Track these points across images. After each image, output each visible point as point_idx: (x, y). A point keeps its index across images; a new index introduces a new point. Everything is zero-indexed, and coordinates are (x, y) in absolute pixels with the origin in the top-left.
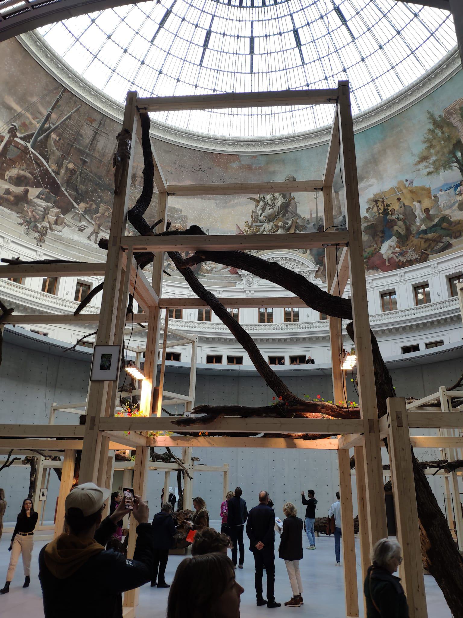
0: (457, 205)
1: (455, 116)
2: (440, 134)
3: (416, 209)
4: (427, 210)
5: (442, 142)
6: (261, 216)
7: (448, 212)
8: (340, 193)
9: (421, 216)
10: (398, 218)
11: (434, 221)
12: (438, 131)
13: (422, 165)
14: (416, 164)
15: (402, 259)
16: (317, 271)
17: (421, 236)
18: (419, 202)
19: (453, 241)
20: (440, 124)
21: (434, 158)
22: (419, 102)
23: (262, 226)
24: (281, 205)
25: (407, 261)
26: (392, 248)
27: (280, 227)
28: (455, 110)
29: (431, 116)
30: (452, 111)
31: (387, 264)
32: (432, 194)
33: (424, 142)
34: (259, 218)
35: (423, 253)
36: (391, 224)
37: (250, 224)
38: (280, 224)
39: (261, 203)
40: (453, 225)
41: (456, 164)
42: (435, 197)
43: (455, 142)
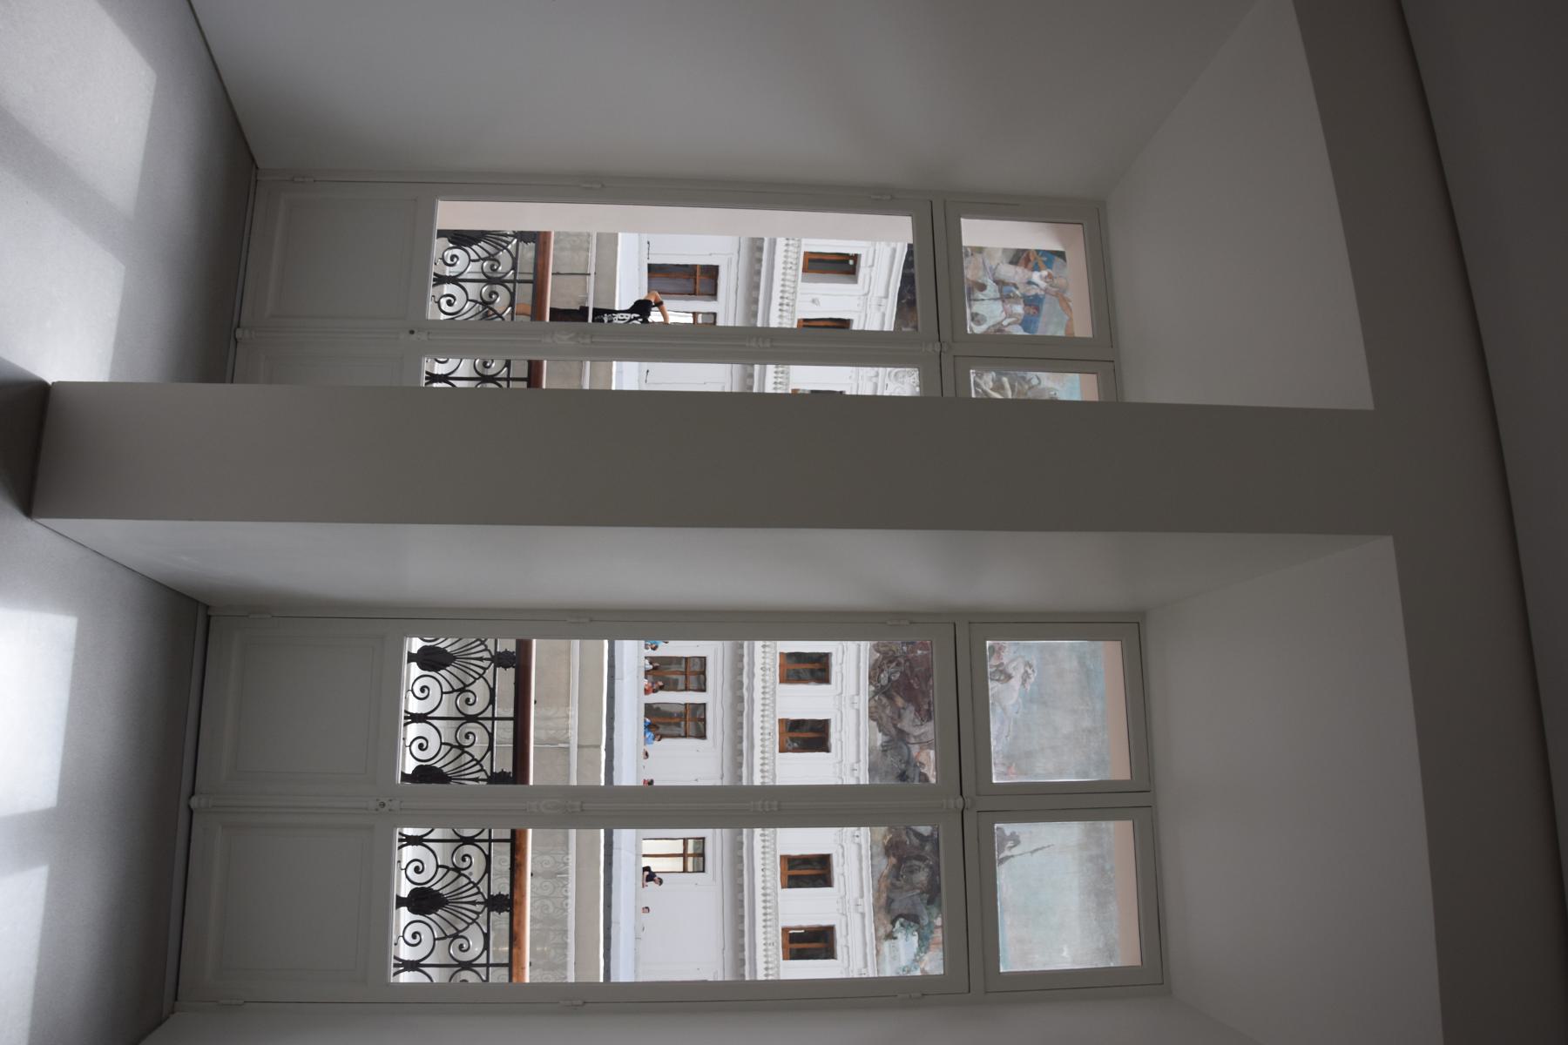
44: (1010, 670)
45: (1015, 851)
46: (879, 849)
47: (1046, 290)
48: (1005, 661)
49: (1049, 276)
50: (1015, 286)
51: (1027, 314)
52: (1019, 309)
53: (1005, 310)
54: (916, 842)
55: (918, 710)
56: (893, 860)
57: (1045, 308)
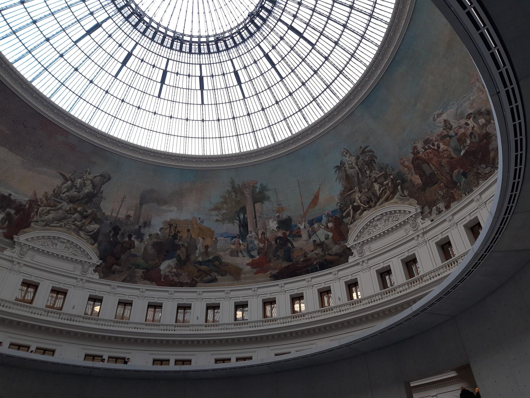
0: (229, 251)
1: (248, 190)
2: (234, 197)
3: (199, 243)
4: (207, 247)
6: (64, 193)
7: (221, 254)
8: (144, 206)
10: (183, 245)
12: (233, 194)
13: (214, 213)
14: (210, 210)
15: (176, 279)
16: (98, 266)
17: (196, 265)
18: (203, 239)
19: (219, 277)
20: (236, 190)
21: (224, 211)
22: (228, 169)
23: (61, 203)
24: (88, 193)
25: (180, 282)
26: (170, 268)
27: (78, 212)
29: (233, 183)
31: (162, 280)
32: (215, 236)
33: (221, 197)
34: (61, 195)
35: (193, 279)
36: (178, 247)
37: (49, 196)
38: (79, 209)
39: (69, 183)
41: (237, 222)
42: (216, 239)
44: (442, 124)
47: (305, 222)
50: (308, 231)
51: (317, 222)
52: (316, 226)
53: (319, 230)
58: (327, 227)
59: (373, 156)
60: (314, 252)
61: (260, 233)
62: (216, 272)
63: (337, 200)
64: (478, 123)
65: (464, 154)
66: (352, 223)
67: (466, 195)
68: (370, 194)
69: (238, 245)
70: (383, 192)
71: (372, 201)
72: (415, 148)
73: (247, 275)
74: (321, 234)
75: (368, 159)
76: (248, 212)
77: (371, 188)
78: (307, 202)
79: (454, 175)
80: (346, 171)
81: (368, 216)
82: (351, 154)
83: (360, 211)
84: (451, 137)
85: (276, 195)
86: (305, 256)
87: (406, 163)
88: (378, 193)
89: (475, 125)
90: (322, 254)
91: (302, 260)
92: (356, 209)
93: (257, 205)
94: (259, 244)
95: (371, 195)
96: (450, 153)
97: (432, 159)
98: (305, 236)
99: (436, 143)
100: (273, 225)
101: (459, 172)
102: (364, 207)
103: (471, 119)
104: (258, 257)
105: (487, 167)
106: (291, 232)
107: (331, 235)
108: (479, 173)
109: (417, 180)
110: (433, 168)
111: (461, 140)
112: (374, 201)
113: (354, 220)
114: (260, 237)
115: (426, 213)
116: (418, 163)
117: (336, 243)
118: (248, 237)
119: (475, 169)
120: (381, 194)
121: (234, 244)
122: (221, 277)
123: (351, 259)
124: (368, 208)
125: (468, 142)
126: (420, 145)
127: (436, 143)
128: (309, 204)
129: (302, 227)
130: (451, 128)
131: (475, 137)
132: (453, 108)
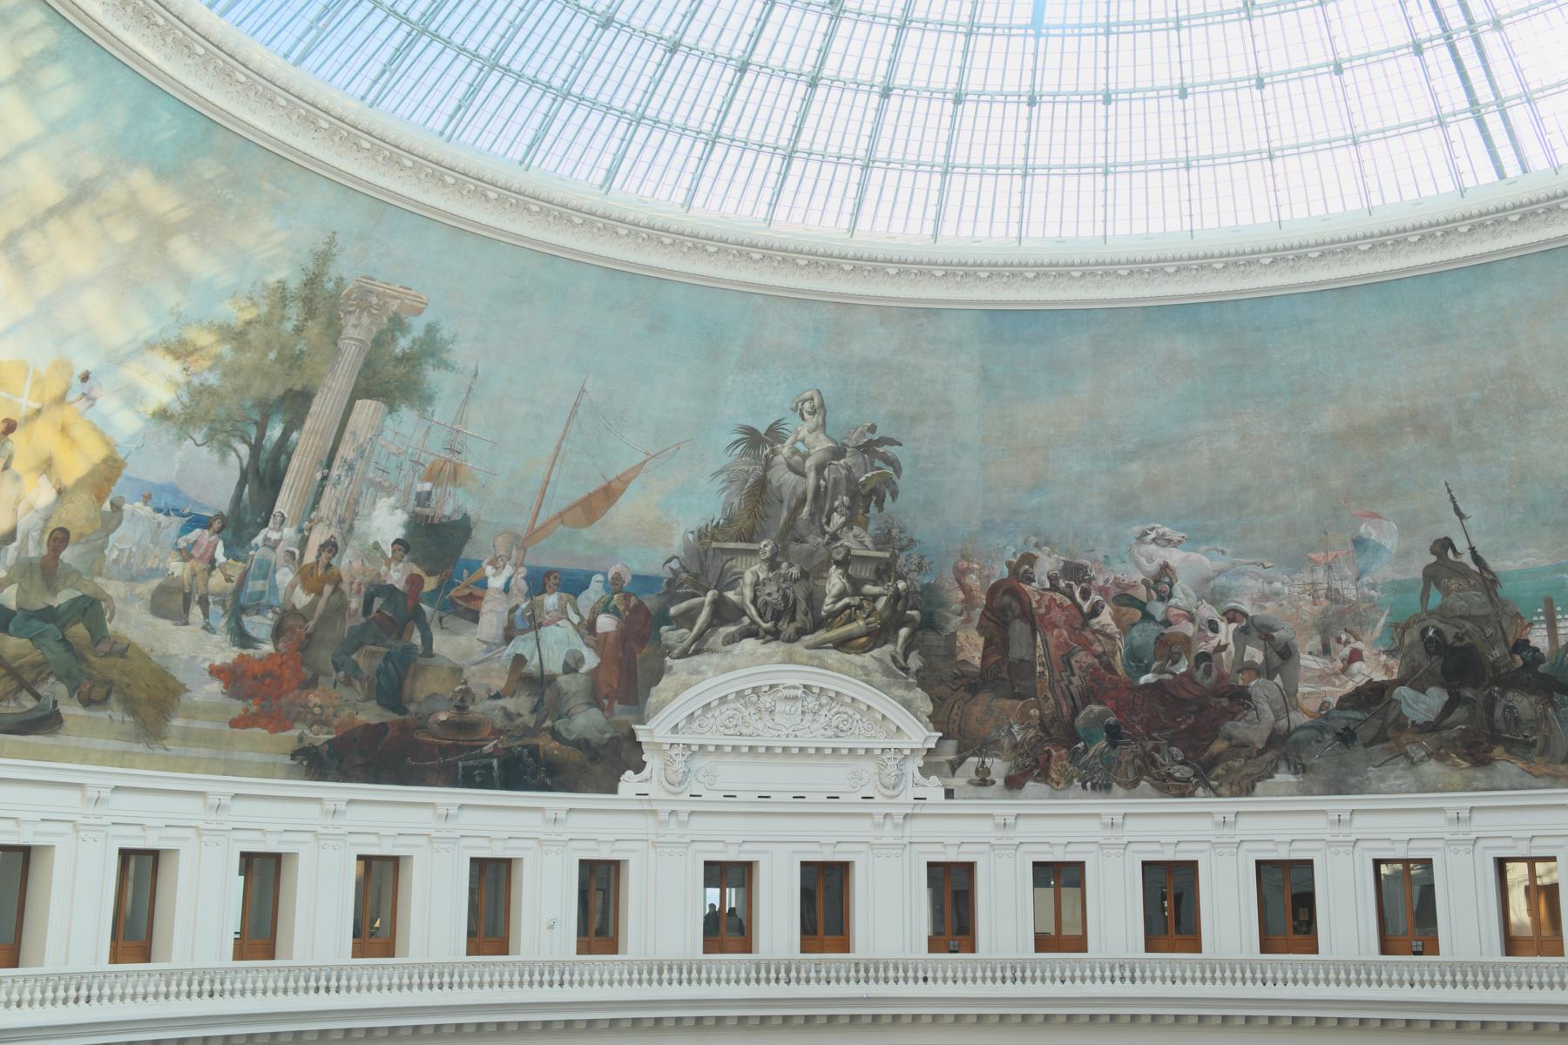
0: (155, 583)
1: (366, 320)
2: (289, 326)
5: (272, 355)
7: (114, 589)
9: (31, 545)
11: (55, 593)
12: (294, 312)
19: (71, 710)
22: (347, 188)
28: (382, 307)
29: (324, 258)
30: (374, 300)
32: (115, 492)
40: (104, 647)
41: (244, 450)
42: (117, 507)
43: (298, 387)
44: (1153, 568)
45: (1461, 544)
46: (1480, 774)
47: (516, 566)
48: (1139, 577)
49: (493, 563)
50: (512, 611)
52: (551, 600)
53: (554, 622)
54: (1460, 713)
55: (1233, 716)
56: (1498, 751)
57: (546, 563)
58: (591, 626)
59: (889, 482)
60: (501, 702)
61: (318, 537)
62: (66, 677)
63: (677, 545)
64: (1240, 650)
65: (1147, 685)
66: (685, 654)
67: (1084, 787)
68: (800, 591)
69: (200, 566)
70: (845, 614)
71: (793, 619)
72: (1029, 559)
73: (197, 724)
74: (557, 645)
75: (864, 479)
76: (308, 424)
77: (812, 574)
78: (567, 492)
79: (1082, 714)
80: (767, 466)
81: (753, 665)
82: (824, 424)
83: (732, 629)
84: (1147, 616)
85: (466, 402)
86: (461, 708)
87: (972, 580)
88: (828, 605)
89: (1232, 647)
90: (530, 720)
91: (443, 717)
92: (723, 613)
93: (366, 409)
94: (292, 587)
95: (800, 595)
96: (1114, 654)
97: (1055, 626)
98: (491, 620)
99: (1095, 597)
100: (386, 523)
101: (1101, 716)
102: (753, 622)
103: (1234, 626)
104: (268, 648)
105: (1182, 763)
106: (447, 584)
107: (591, 660)
108: (1154, 762)
109: (972, 647)
110: (1040, 651)
111: (1169, 647)
112: (798, 624)
113: (699, 646)
114: (310, 557)
115: (942, 759)
116: (1006, 607)
117: (595, 697)
118: (259, 539)
119: (1151, 743)
120: (834, 615)
121: (186, 555)
122: (79, 710)
123: (629, 783)
124: (767, 632)
125: (1182, 667)
126: (1047, 564)
127: (1095, 597)
128: (565, 504)
129: (496, 582)
130: (1164, 597)
131: (1208, 672)
132: (1211, 559)
